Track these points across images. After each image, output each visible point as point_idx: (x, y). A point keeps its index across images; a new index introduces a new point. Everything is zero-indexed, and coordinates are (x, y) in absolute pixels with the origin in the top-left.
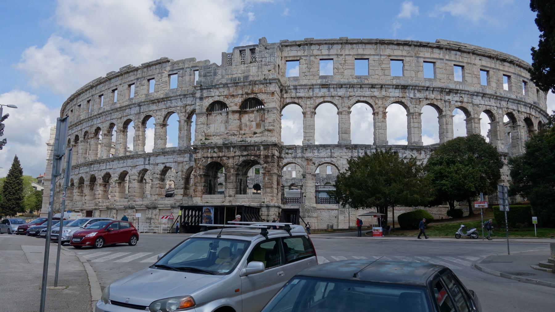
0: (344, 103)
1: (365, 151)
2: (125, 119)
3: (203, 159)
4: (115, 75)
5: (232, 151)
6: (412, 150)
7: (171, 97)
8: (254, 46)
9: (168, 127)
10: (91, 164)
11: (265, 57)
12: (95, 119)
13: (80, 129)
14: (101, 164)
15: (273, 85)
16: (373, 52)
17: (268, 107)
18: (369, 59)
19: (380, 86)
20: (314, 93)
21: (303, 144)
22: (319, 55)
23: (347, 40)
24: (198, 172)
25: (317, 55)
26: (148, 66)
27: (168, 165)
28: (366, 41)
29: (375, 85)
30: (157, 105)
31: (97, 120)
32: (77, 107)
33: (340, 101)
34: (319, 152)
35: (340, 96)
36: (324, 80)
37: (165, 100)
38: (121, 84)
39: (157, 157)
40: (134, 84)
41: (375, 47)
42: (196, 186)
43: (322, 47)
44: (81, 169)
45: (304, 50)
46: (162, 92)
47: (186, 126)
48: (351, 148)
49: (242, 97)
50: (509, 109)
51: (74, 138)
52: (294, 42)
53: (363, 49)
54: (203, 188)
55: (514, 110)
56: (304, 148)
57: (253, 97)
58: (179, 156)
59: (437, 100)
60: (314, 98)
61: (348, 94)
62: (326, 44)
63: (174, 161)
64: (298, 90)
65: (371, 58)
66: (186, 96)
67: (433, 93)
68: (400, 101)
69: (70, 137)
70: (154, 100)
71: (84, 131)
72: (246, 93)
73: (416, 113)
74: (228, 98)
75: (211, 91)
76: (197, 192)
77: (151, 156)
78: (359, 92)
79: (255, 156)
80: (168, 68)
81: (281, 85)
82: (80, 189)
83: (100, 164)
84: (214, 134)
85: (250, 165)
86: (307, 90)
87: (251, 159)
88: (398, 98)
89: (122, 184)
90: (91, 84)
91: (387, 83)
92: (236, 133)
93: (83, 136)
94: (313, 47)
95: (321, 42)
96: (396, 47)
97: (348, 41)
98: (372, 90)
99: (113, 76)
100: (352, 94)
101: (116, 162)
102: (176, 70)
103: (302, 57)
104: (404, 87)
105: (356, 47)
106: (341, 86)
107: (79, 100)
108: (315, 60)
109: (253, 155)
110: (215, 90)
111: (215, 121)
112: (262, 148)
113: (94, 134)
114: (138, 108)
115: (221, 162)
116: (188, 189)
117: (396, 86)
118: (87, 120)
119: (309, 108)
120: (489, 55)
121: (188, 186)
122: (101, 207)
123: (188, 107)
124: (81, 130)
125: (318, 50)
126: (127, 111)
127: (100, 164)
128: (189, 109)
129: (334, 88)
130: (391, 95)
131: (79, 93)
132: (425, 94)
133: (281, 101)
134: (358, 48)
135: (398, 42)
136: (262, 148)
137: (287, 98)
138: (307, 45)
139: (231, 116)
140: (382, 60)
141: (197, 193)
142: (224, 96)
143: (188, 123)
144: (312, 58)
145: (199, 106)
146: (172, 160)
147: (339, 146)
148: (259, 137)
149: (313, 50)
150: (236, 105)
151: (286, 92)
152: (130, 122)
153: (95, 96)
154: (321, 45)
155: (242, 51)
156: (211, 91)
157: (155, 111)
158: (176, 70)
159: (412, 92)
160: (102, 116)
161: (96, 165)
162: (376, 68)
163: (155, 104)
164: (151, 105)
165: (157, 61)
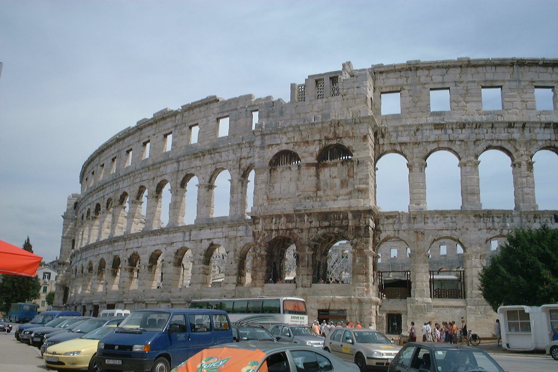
2: (159, 180)
3: (266, 232)
4: (147, 123)
5: (305, 221)
7: (221, 148)
8: (336, 72)
9: (215, 190)
10: (115, 241)
11: (352, 88)
12: (120, 181)
13: (101, 195)
14: (127, 242)
15: (365, 125)
16: (508, 78)
17: (358, 157)
18: (503, 87)
20: (425, 134)
21: (409, 209)
23: (469, 61)
24: (258, 251)
25: (425, 84)
26: (189, 108)
27: (215, 242)
29: (514, 124)
30: (202, 159)
31: (123, 183)
32: (99, 167)
33: (463, 147)
35: (462, 141)
36: (438, 118)
37: (212, 152)
38: (154, 135)
39: (200, 230)
40: (171, 133)
41: (511, 69)
42: (255, 270)
43: (432, 72)
44: (101, 248)
45: (407, 78)
46: (207, 142)
47: (240, 187)
48: (481, 215)
49: (320, 144)
51: (95, 207)
52: (392, 65)
53: (493, 73)
54: (264, 274)
56: (412, 216)
57: (335, 143)
58: (230, 229)
60: (424, 143)
61: (473, 137)
62: (438, 67)
63: (224, 236)
64: (400, 133)
65: (506, 85)
66: (241, 146)
68: (553, 145)
69: (89, 207)
70: (197, 153)
71: (107, 197)
72: (325, 137)
74: (299, 146)
75: (275, 138)
76: (256, 279)
77: (192, 230)
78: (489, 134)
79: (341, 227)
80: (216, 110)
81: (376, 126)
82: (101, 275)
83: (125, 241)
84: (280, 196)
85: (333, 240)
86: (413, 132)
87: (335, 232)
88: (549, 141)
89: (153, 269)
90: (118, 137)
91: (532, 120)
92: (311, 194)
93: (105, 205)
94: (419, 72)
95: (432, 65)
96: (542, 69)
97: (470, 63)
98: (510, 130)
99: (144, 124)
100: (479, 137)
101: (145, 239)
102: (227, 111)
103: (404, 87)
107: (102, 159)
108: (423, 90)
109: (337, 227)
110: (281, 136)
111: (281, 178)
112: (350, 216)
113: (119, 201)
114: (175, 165)
115: (291, 237)
116: (242, 276)
117: (546, 124)
118: (111, 183)
119: (417, 157)
121: (243, 271)
122: (126, 300)
123: (243, 161)
124: (104, 196)
125: (427, 76)
126: (162, 169)
127: (125, 241)
128: (245, 163)
129: (453, 130)
130: (539, 137)
131: (102, 149)
134: (485, 71)
135: (545, 62)
136: (350, 216)
137: (383, 144)
138: (411, 70)
139: (304, 171)
140: (522, 87)
141: (257, 282)
142: (295, 144)
143: (242, 183)
144: (418, 87)
145: (258, 158)
146: (220, 235)
147: (462, 212)
148: (346, 200)
149: (420, 76)
150: (312, 154)
151: (383, 136)
152: (165, 184)
153: (122, 152)
154: (431, 69)
155: (317, 80)
156: (275, 138)
157: (198, 168)
158: (227, 111)
160: (130, 177)
161: (120, 243)
162: (515, 99)
163: (198, 159)
164: (193, 160)
165: (202, 100)
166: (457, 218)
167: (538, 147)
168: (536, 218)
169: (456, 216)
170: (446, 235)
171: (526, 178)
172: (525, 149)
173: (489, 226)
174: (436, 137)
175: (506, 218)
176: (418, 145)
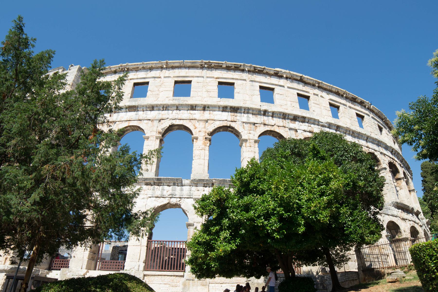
19: (202, 108)
20: (119, 117)
22: (133, 79)
29: (196, 106)
35: (150, 120)
48: (152, 183)
50: (370, 148)
55: (376, 151)
59: (278, 126)
61: (160, 117)
73: (251, 140)
97: (168, 64)
100: (164, 117)
104: (235, 110)
106: (152, 108)
117: (223, 108)
120: (337, 91)
132: (262, 120)
154: (138, 70)
159: (246, 115)
171: (201, 151)
172: (203, 126)
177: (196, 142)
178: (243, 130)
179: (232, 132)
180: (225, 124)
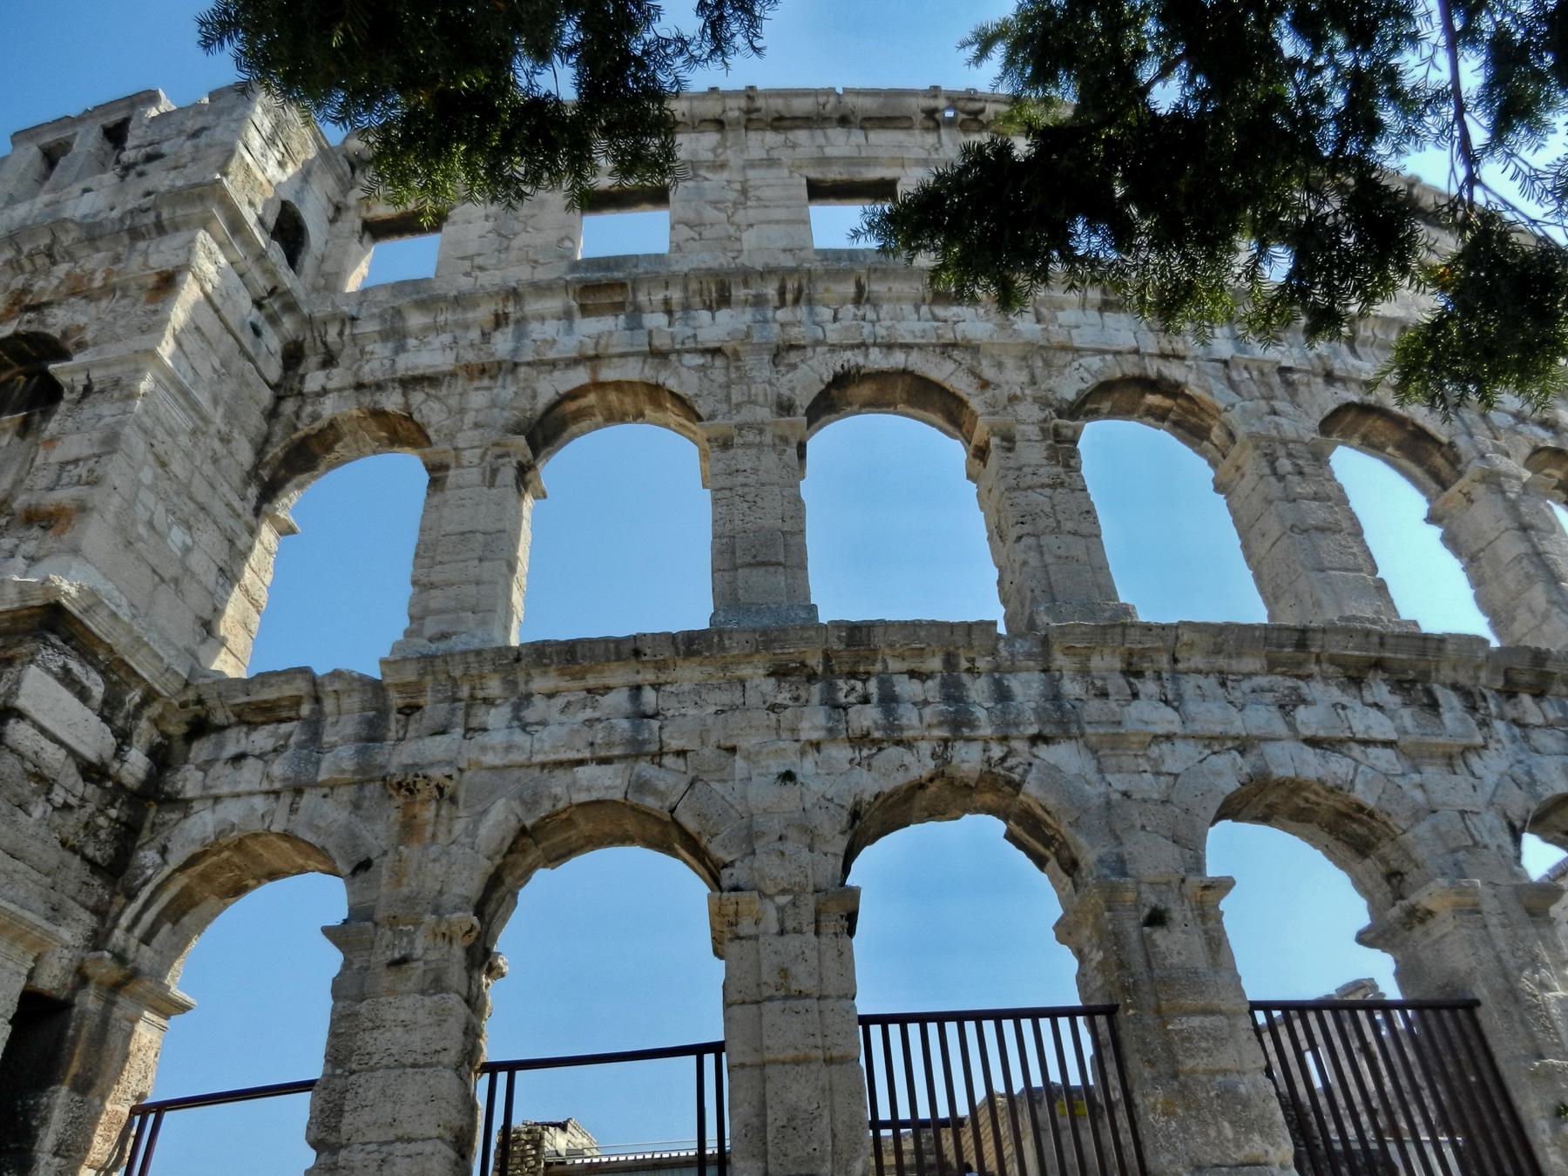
0: (744, 378)
1: (944, 684)
6: (1354, 677)
28: (869, 105)
33: (718, 375)
34: (530, 715)
35: (716, 352)
48: (815, 662)
56: (396, 700)
61: (774, 333)
67: (1353, 352)
86: (475, 334)
88: (1133, 358)
105: (813, 139)
119: (477, 425)
129: (669, 312)
133: (272, 414)
137: (324, 392)
151: (329, 361)
166: (668, 688)
167: (1086, 375)
168: (1139, 674)
169: (663, 678)
170: (594, 796)
173: (867, 723)
174: (587, 340)
175: (965, 678)
176: (492, 378)
177: (1010, 450)
178: (1233, 398)
179: (1158, 416)
180: (1130, 367)
